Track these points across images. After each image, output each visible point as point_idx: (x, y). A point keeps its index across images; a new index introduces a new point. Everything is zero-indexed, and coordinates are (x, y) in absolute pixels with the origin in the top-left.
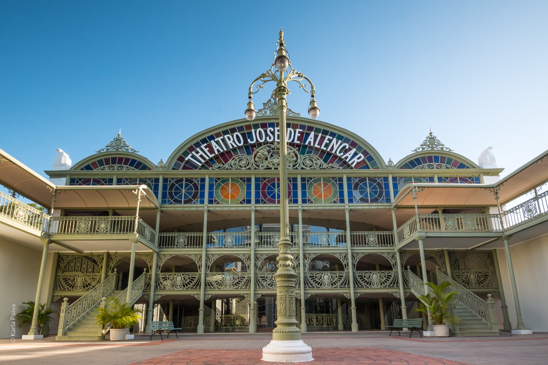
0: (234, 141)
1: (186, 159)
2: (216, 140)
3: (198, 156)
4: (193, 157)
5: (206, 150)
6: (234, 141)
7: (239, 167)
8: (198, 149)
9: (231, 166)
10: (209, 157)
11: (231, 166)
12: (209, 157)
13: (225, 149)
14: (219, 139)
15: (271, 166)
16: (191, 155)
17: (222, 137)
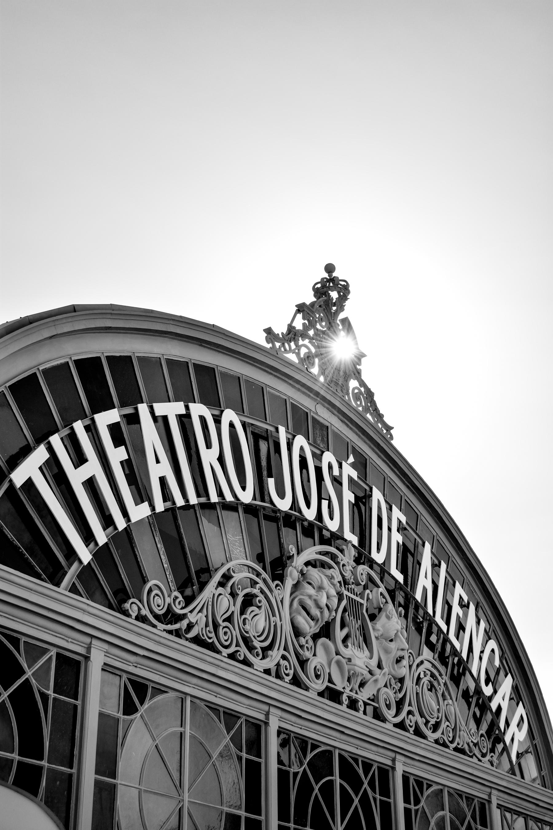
0: (221, 459)
1: (18, 477)
2: (161, 409)
3: (76, 477)
4: (54, 471)
5: (117, 455)
6: (221, 459)
7: (243, 650)
8: (79, 427)
9: (216, 626)
10: (125, 514)
11: (216, 626)
12: (125, 514)
13: (193, 500)
14: (171, 409)
15: (339, 684)
16: (40, 455)
17: (178, 408)
